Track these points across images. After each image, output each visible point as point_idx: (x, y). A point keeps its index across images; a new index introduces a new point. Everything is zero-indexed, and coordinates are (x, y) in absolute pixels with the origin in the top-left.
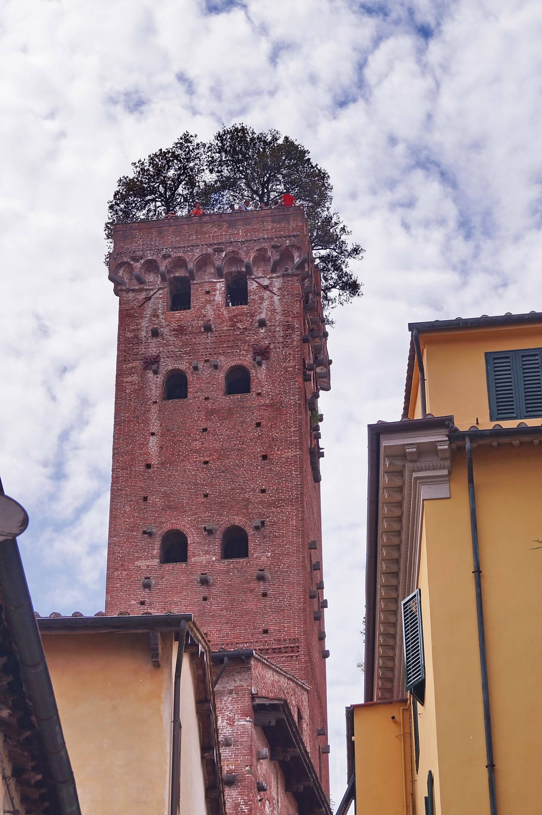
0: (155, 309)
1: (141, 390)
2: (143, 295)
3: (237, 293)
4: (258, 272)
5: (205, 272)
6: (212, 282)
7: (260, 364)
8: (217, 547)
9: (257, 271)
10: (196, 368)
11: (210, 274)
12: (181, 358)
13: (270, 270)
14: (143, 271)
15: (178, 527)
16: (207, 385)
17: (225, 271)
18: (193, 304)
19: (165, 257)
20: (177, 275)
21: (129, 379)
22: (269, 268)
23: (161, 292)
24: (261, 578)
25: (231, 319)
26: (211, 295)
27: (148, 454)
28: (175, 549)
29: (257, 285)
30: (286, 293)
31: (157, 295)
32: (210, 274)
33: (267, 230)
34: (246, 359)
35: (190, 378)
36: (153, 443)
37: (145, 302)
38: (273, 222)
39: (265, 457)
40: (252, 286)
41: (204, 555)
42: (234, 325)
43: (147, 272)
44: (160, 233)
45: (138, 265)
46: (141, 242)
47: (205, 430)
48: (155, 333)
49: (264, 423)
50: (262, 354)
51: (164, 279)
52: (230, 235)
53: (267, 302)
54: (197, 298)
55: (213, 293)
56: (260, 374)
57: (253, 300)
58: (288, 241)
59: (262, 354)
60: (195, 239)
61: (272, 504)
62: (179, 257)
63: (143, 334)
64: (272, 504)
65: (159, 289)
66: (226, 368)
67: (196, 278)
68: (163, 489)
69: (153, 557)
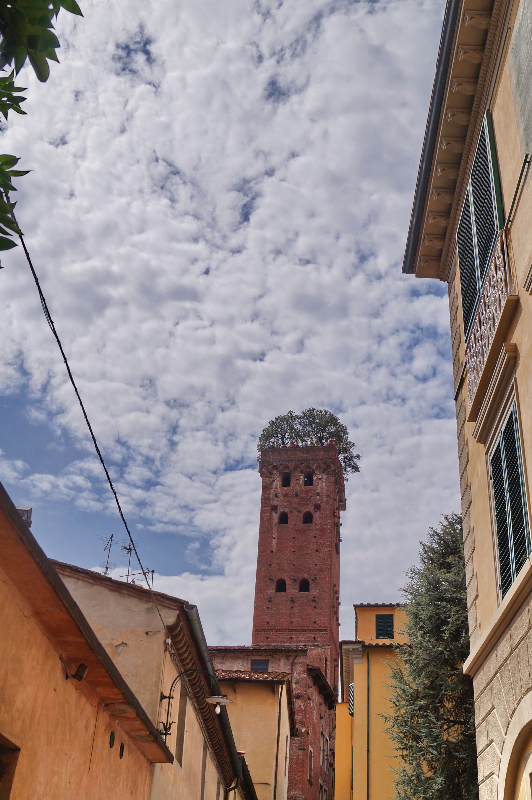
1: (270, 519)
7: (316, 511)
8: (297, 587)
10: (292, 512)
16: (296, 519)
17: (304, 471)
18: (291, 484)
19: (281, 465)
21: (266, 514)
22: (322, 470)
24: (314, 601)
25: (306, 492)
27: (272, 546)
28: (281, 586)
34: (311, 509)
35: (289, 516)
36: (274, 542)
38: (324, 451)
39: (317, 551)
40: (315, 478)
41: (292, 590)
45: (270, 467)
47: (294, 538)
48: (276, 496)
49: (317, 536)
50: (318, 507)
54: (293, 482)
56: (316, 516)
59: (318, 507)
61: (319, 570)
64: (319, 570)
66: (303, 512)
68: (278, 561)
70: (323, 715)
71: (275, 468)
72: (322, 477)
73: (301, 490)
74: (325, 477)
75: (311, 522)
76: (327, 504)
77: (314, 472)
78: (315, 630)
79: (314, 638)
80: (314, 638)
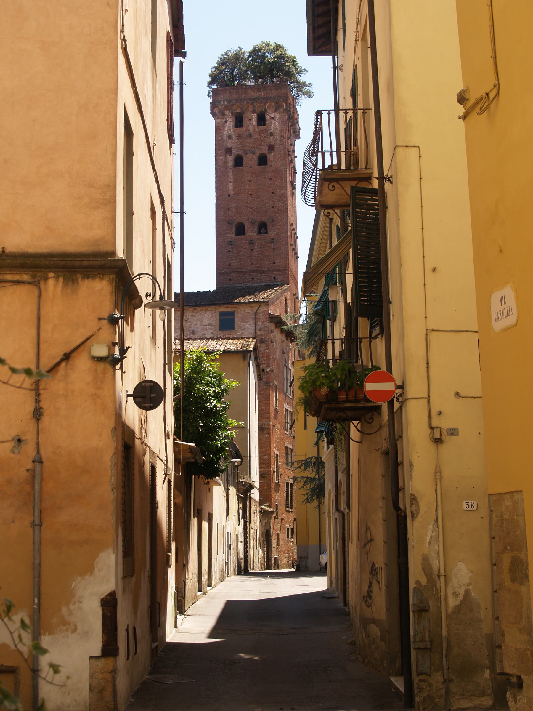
3: (262, 120)
4: (269, 111)
7: (271, 153)
8: (256, 230)
12: (241, 150)
15: (242, 221)
16: (251, 160)
18: (244, 125)
22: (274, 110)
25: (259, 132)
26: (251, 120)
28: (240, 230)
34: (265, 151)
35: (244, 158)
36: (231, 186)
38: (276, 89)
40: (268, 117)
41: (251, 233)
42: (260, 135)
44: (230, 93)
46: (222, 97)
47: (250, 181)
50: (271, 148)
51: (232, 113)
54: (246, 123)
56: (271, 157)
63: (225, 137)
68: (235, 205)
69: (232, 233)
70: (285, 351)
71: (226, 108)
72: (275, 116)
73: (254, 130)
74: (278, 116)
75: (267, 165)
76: (280, 145)
77: (266, 111)
78: (274, 271)
79: (274, 278)
80: (274, 278)
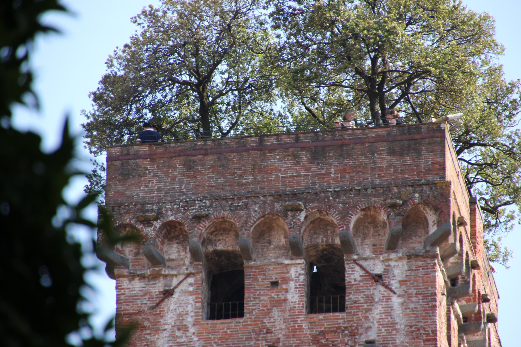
0: (180, 315)
2: (159, 286)
5: (270, 243)
6: (281, 264)
9: (362, 245)
11: (278, 247)
13: (384, 246)
14: (158, 241)
18: (248, 306)
19: (198, 218)
20: (220, 247)
23: (191, 280)
29: (362, 273)
30: (413, 291)
31: (184, 286)
32: (278, 247)
33: (380, 169)
37: (162, 301)
38: (392, 152)
40: (353, 275)
43: (166, 241)
45: (149, 231)
46: (154, 185)
51: (195, 255)
52: (314, 176)
53: (380, 307)
55: (284, 286)
57: (355, 302)
58: (417, 195)
60: (252, 183)
62: (223, 218)
65: (188, 275)
67: (254, 256)
73: (294, 332)
